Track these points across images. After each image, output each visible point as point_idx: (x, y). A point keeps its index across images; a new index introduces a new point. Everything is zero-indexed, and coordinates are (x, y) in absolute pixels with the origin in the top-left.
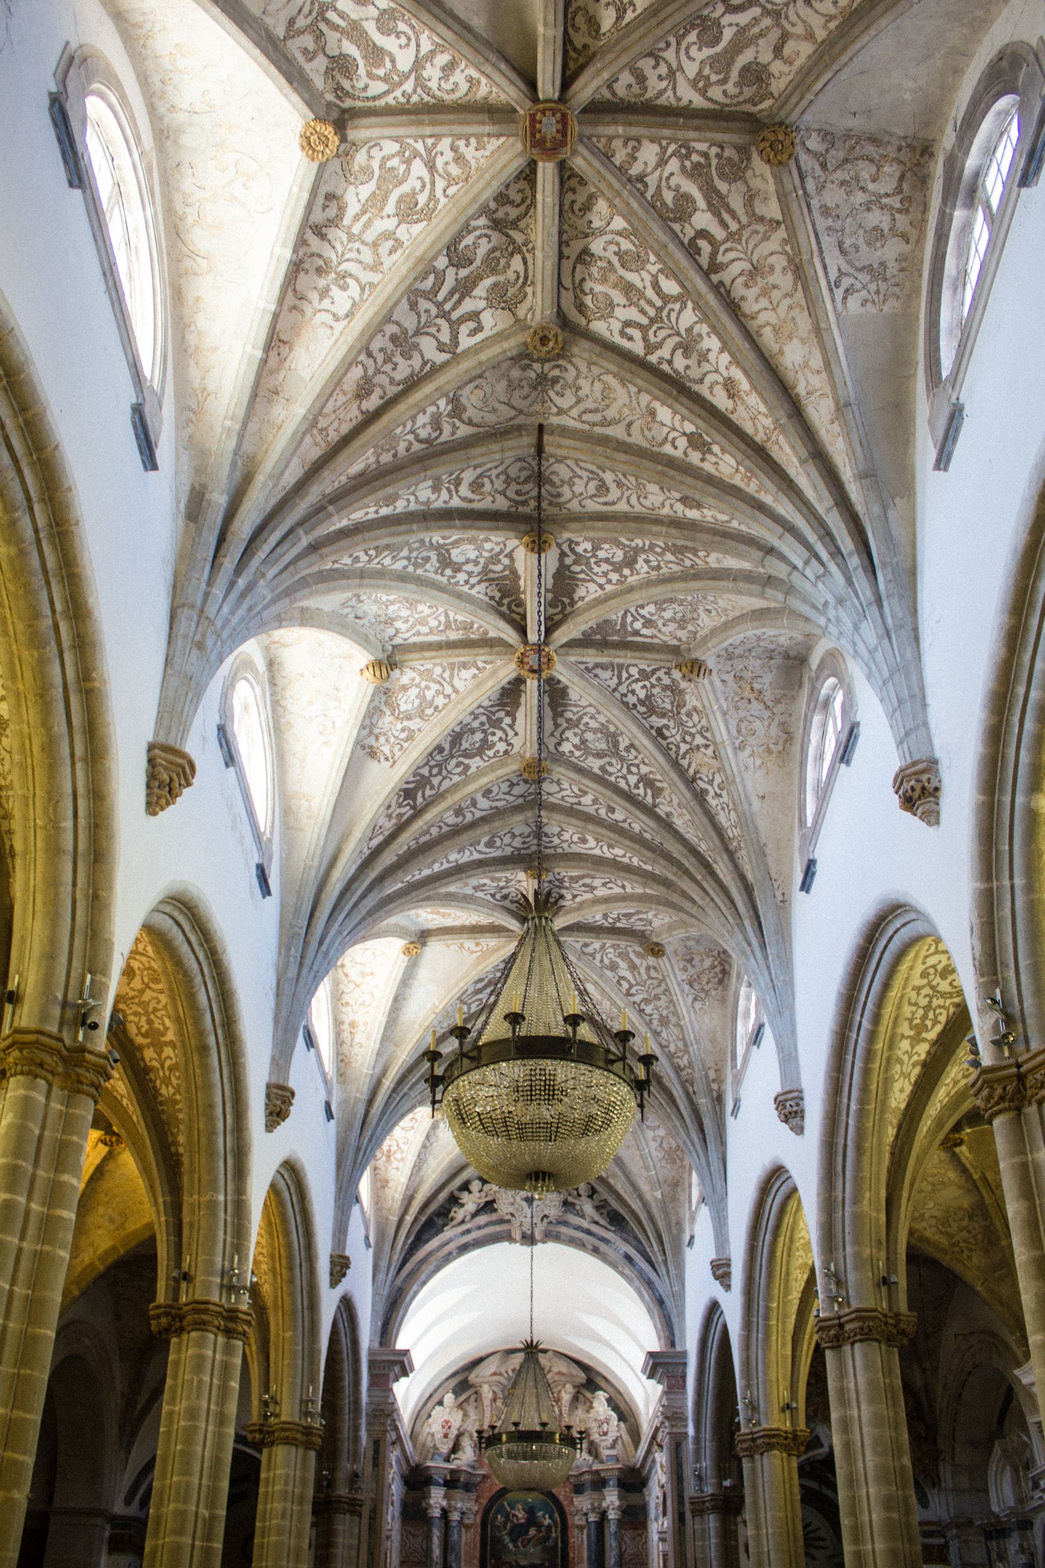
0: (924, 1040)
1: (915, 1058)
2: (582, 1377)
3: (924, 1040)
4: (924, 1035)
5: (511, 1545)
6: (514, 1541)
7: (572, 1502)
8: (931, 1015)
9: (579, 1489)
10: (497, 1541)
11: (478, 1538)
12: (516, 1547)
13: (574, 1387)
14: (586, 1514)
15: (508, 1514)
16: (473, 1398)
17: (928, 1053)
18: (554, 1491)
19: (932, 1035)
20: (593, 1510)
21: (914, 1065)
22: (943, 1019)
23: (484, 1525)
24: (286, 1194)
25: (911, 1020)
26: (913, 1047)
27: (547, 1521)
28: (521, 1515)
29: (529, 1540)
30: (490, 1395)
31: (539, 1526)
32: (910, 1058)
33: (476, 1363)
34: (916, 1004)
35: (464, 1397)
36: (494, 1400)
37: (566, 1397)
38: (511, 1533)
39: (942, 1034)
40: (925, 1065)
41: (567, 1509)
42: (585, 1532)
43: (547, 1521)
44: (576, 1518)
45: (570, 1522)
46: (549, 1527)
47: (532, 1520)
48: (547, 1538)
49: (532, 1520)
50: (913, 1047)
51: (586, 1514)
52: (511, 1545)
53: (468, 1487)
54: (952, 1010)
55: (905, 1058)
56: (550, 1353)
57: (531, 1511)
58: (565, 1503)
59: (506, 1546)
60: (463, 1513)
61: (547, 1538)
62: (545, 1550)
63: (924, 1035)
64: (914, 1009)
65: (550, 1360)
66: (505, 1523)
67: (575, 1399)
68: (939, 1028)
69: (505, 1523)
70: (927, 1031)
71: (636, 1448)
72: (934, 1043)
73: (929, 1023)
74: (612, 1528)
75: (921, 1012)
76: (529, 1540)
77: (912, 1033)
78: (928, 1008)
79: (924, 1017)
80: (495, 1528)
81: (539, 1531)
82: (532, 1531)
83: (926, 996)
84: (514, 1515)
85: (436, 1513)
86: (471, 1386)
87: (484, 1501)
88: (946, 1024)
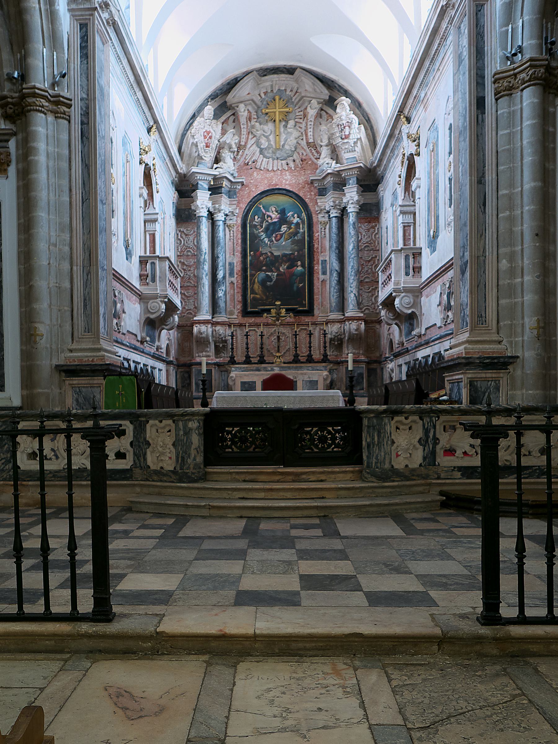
2: (325, 93)
5: (266, 240)
6: (269, 237)
7: (317, 203)
9: (322, 192)
10: (254, 237)
11: (239, 236)
13: (319, 103)
14: (328, 212)
15: (264, 215)
16: (232, 118)
18: (301, 194)
20: (334, 207)
23: (244, 226)
27: (296, 220)
28: (275, 216)
29: (281, 235)
30: (246, 113)
31: (289, 223)
33: (233, 84)
35: (223, 118)
36: (250, 119)
37: (312, 112)
38: (267, 230)
41: (312, 209)
42: (328, 226)
43: (296, 220)
44: (320, 216)
45: (315, 219)
46: (298, 224)
47: (283, 220)
48: (296, 233)
49: (283, 220)
51: (328, 212)
53: (231, 194)
56: (296, 73)
57: (282, 212)
58: (310, 205)
59: (262, 241)
60: (227, 215)
61: (296, 233)
62: (293, 242)
65: (297, 81)
66: (262, 222)
67: (319, 116)
69: (262, 222)
71: (373, 152)
74: (352, 218)
76: (281, 235)
80: (253, 227)
81: (290, 228)
82: (284, 228)
84: (268, 216)
85: (204, 213)
86: (229, 108)
87: (243, 206)
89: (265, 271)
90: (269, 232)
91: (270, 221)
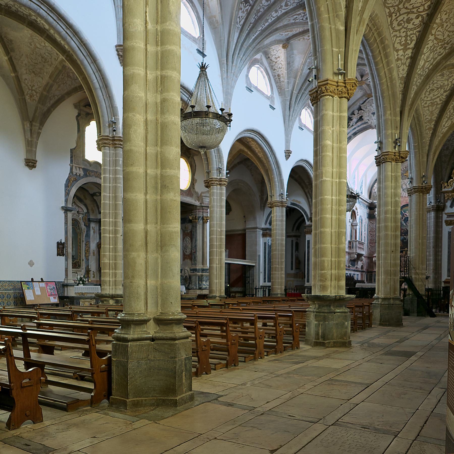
0: (409, 48)
1: (407, 56)
3: (409, 48)
4: (408, 47)
5: (404, 224)
8: (409, 38)
12: (406, 224)
17: (412, 53)
19: (412, 45)
21: (407, 59)
22: (415, 38)
24: (256, 138)
25: (400, 43)
26: (405, 53)
32: (404, 57)
34: (400, 36)
39: (416, 44)
40: (411, 58)
50: (405, 53)
52: (404, 224)
54: (417, 34)
55: (402, 57)
63: (408, 47)
64: (400, 38)
68: (414, 42)
70: (409, 45)
72: (413, 49)
73: (409, 42)
75: (403, 39)
77: (402, 47)
78: (406, 36)
79: (406, 40)
83: (403, 32)
88: (417, 40)
89: (403, 236)
90: (405, 221)
91: (406, 216)
